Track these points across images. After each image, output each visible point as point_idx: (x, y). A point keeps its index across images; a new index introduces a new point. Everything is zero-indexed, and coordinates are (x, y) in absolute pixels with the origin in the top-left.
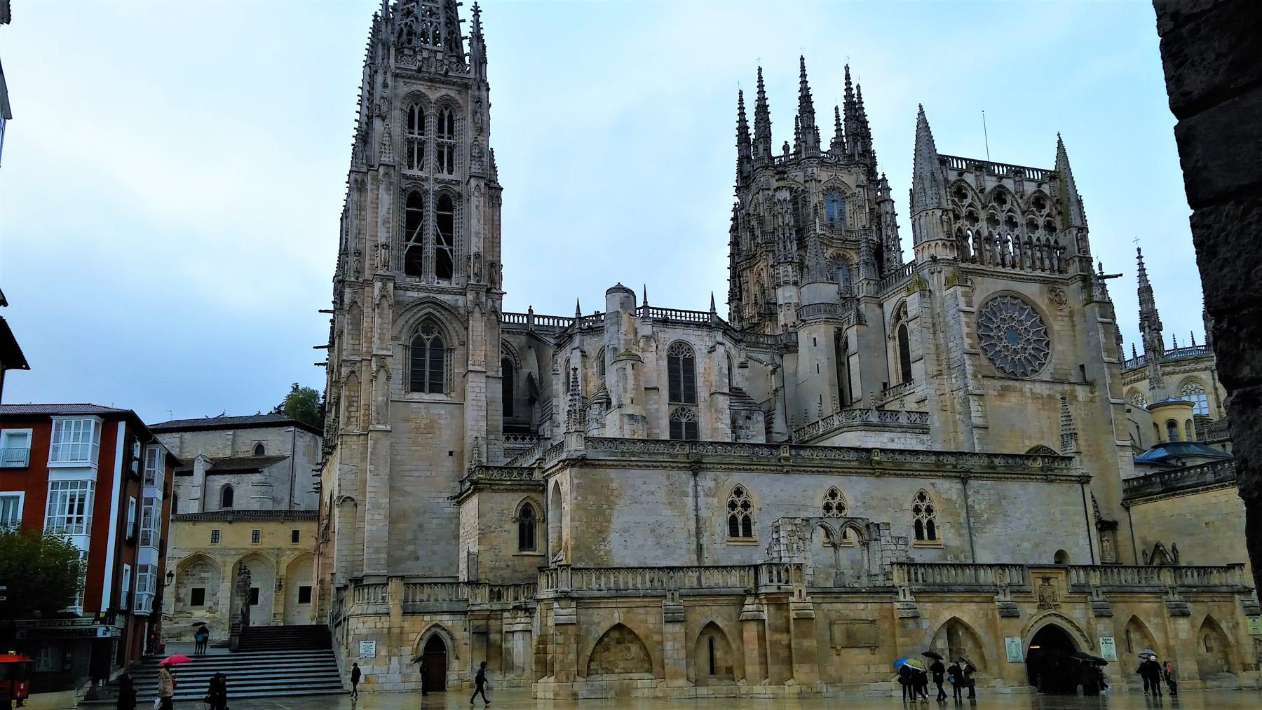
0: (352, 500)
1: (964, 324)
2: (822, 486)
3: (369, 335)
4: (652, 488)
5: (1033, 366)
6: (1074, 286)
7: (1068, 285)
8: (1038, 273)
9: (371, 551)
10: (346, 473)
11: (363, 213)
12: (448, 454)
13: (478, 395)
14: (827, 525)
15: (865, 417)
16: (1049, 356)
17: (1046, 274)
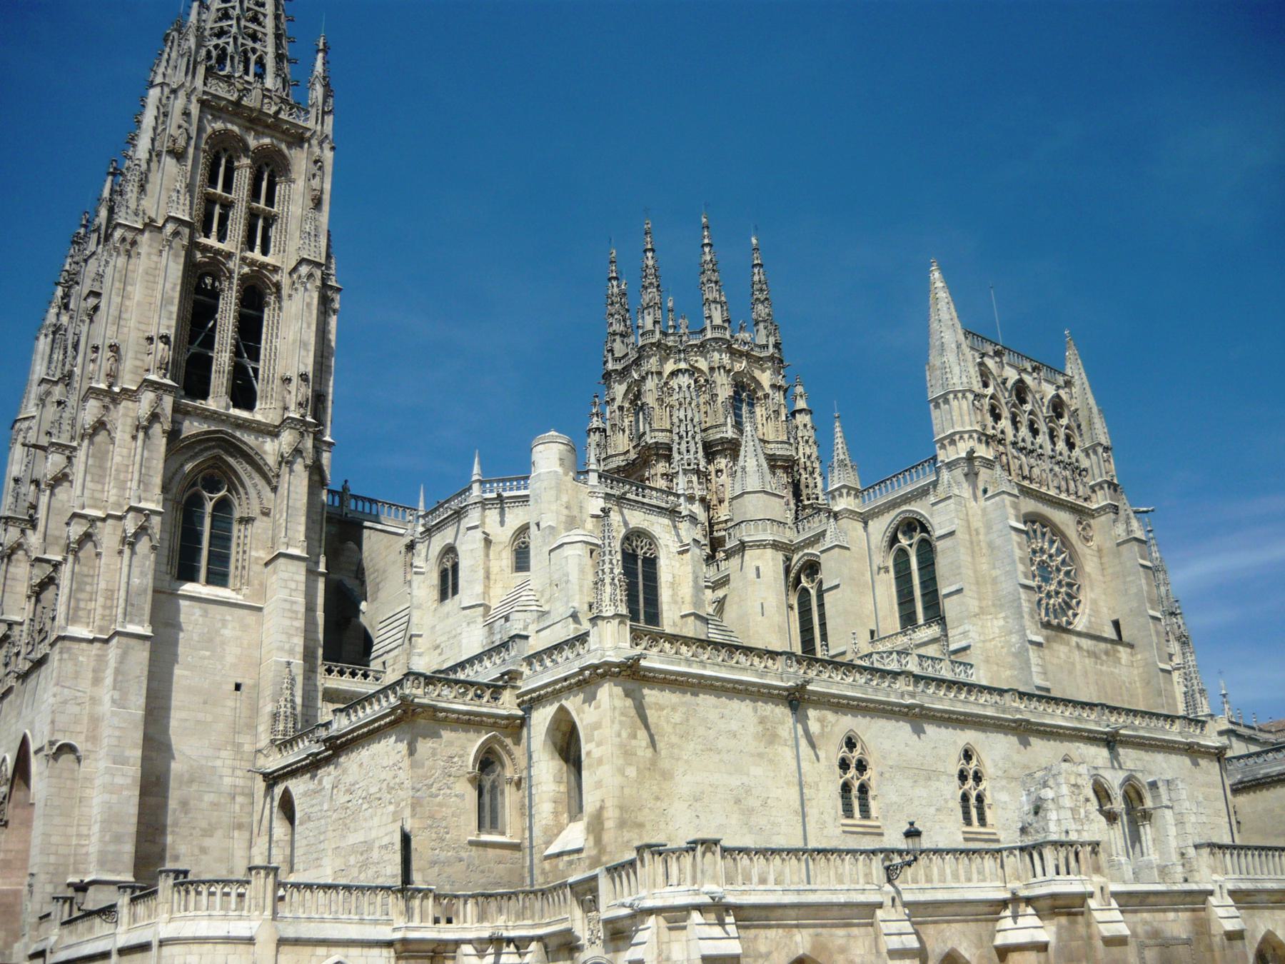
0: (68, 748)
1: (1015, 545)
2: (955, 742)
3: (122, 476)
4: (734, 725)
5: (1067, 616)
6: (1103, 518)
7: (1093, 517)
8: (1063, 496)
9: (107, 838)
10: (65, 702)
11: (129, 288)
12: (233, 687)
13: (293, 594)
14: (1102, 780)
15: (904, 662)
16: (1081, 606)
17: (1071, 499)
